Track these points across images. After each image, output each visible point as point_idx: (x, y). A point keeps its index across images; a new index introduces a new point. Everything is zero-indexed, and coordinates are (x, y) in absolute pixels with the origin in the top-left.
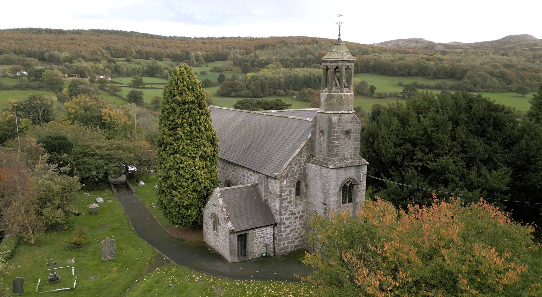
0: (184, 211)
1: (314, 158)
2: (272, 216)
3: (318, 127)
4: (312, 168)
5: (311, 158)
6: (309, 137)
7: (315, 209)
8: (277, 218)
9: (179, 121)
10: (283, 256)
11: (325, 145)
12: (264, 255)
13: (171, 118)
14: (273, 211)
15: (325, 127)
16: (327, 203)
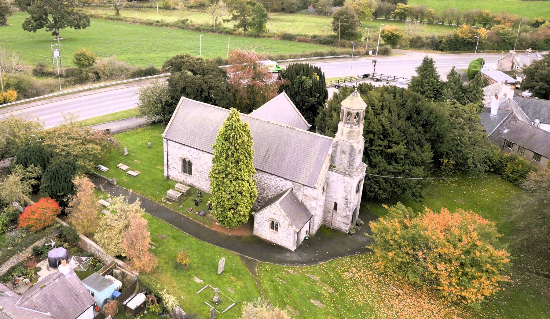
0: (242, 218)
1: (336, 169)
2: (308, 211)
3: (339, 148)
4: (334, 176)
5: (332, 167)
6: (330, 152)
7: (335, 201)
8: (313, 212)
9: (241, 157)
10: (315, 235)
11: (346, 161)
12: (307, 238)
13: (235, 155)
14: (308, 207)
15: (347, 150)
16: (348, 198)
